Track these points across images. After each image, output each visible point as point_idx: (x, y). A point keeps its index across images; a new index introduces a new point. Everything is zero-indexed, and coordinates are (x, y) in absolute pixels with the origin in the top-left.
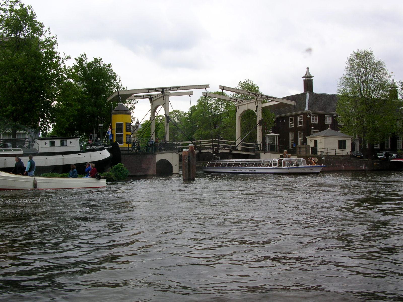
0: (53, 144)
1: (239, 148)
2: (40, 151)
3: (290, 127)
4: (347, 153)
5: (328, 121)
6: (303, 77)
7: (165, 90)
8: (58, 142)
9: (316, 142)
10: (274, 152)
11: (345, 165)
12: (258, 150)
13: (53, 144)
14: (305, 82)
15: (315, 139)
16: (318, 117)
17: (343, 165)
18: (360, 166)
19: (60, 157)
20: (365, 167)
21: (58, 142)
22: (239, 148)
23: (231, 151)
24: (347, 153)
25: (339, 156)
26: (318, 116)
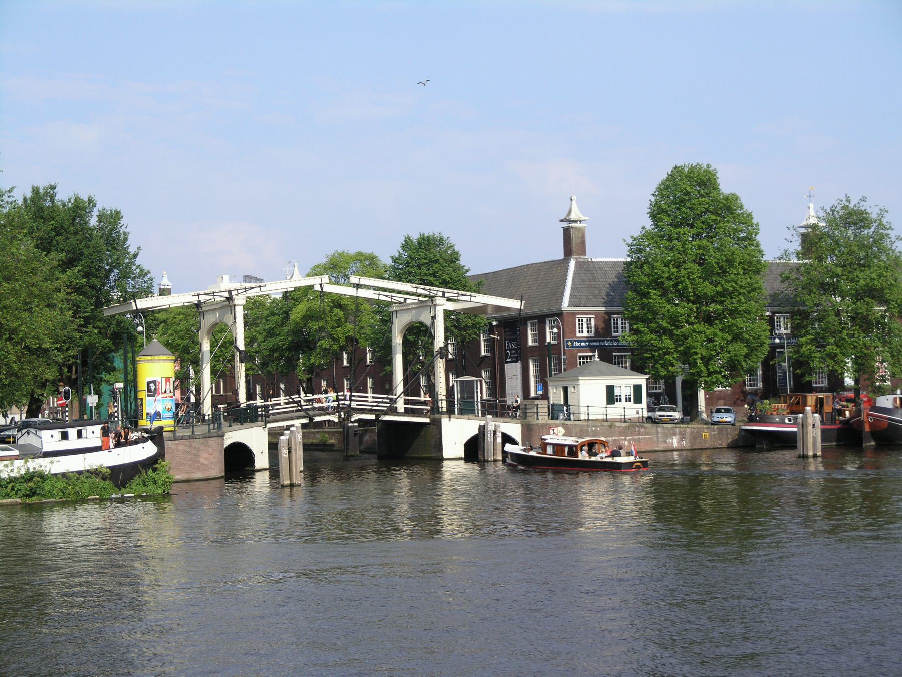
0: (65, 436)
1: (401, 406)
2: (45, 449)
3: (530, 343)
4: (638, 413)
5: (620, 330)
6: (562, 221)
7: (233, 293)
8: (72, 432)
9: (565, 389)
10: (470, 416)
11: (629, 441)
12: (439, 412)
13: (65, 436)
14: (567, 232)
15: (565, 384)
16: (593, 320)
17: (625, 440)
18: (665, 442)
19: (80, 457)
20: (679, 443)
21: (72, 432)
22: (401, 406)
23: (377, 416)
24: (638, 413)
25: (616, 421)
26: (595, 319)
